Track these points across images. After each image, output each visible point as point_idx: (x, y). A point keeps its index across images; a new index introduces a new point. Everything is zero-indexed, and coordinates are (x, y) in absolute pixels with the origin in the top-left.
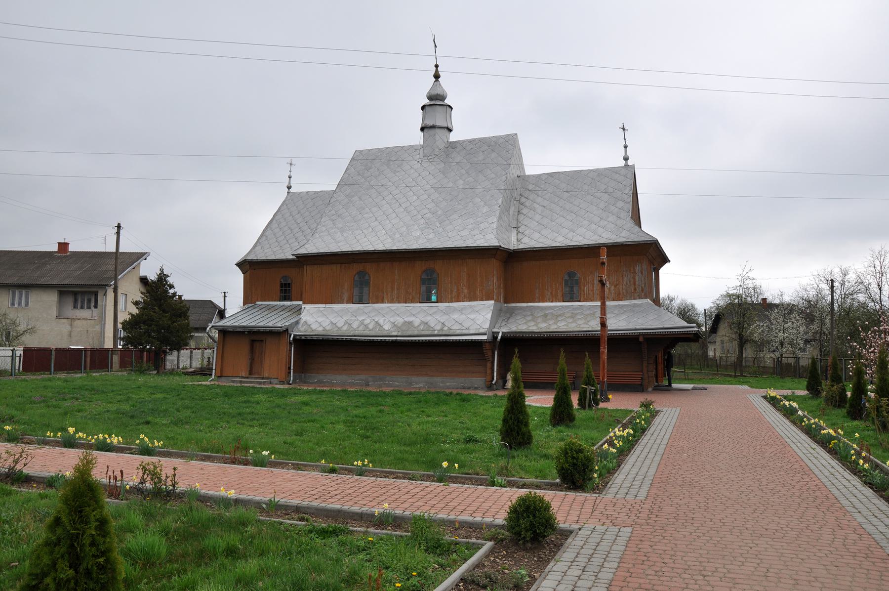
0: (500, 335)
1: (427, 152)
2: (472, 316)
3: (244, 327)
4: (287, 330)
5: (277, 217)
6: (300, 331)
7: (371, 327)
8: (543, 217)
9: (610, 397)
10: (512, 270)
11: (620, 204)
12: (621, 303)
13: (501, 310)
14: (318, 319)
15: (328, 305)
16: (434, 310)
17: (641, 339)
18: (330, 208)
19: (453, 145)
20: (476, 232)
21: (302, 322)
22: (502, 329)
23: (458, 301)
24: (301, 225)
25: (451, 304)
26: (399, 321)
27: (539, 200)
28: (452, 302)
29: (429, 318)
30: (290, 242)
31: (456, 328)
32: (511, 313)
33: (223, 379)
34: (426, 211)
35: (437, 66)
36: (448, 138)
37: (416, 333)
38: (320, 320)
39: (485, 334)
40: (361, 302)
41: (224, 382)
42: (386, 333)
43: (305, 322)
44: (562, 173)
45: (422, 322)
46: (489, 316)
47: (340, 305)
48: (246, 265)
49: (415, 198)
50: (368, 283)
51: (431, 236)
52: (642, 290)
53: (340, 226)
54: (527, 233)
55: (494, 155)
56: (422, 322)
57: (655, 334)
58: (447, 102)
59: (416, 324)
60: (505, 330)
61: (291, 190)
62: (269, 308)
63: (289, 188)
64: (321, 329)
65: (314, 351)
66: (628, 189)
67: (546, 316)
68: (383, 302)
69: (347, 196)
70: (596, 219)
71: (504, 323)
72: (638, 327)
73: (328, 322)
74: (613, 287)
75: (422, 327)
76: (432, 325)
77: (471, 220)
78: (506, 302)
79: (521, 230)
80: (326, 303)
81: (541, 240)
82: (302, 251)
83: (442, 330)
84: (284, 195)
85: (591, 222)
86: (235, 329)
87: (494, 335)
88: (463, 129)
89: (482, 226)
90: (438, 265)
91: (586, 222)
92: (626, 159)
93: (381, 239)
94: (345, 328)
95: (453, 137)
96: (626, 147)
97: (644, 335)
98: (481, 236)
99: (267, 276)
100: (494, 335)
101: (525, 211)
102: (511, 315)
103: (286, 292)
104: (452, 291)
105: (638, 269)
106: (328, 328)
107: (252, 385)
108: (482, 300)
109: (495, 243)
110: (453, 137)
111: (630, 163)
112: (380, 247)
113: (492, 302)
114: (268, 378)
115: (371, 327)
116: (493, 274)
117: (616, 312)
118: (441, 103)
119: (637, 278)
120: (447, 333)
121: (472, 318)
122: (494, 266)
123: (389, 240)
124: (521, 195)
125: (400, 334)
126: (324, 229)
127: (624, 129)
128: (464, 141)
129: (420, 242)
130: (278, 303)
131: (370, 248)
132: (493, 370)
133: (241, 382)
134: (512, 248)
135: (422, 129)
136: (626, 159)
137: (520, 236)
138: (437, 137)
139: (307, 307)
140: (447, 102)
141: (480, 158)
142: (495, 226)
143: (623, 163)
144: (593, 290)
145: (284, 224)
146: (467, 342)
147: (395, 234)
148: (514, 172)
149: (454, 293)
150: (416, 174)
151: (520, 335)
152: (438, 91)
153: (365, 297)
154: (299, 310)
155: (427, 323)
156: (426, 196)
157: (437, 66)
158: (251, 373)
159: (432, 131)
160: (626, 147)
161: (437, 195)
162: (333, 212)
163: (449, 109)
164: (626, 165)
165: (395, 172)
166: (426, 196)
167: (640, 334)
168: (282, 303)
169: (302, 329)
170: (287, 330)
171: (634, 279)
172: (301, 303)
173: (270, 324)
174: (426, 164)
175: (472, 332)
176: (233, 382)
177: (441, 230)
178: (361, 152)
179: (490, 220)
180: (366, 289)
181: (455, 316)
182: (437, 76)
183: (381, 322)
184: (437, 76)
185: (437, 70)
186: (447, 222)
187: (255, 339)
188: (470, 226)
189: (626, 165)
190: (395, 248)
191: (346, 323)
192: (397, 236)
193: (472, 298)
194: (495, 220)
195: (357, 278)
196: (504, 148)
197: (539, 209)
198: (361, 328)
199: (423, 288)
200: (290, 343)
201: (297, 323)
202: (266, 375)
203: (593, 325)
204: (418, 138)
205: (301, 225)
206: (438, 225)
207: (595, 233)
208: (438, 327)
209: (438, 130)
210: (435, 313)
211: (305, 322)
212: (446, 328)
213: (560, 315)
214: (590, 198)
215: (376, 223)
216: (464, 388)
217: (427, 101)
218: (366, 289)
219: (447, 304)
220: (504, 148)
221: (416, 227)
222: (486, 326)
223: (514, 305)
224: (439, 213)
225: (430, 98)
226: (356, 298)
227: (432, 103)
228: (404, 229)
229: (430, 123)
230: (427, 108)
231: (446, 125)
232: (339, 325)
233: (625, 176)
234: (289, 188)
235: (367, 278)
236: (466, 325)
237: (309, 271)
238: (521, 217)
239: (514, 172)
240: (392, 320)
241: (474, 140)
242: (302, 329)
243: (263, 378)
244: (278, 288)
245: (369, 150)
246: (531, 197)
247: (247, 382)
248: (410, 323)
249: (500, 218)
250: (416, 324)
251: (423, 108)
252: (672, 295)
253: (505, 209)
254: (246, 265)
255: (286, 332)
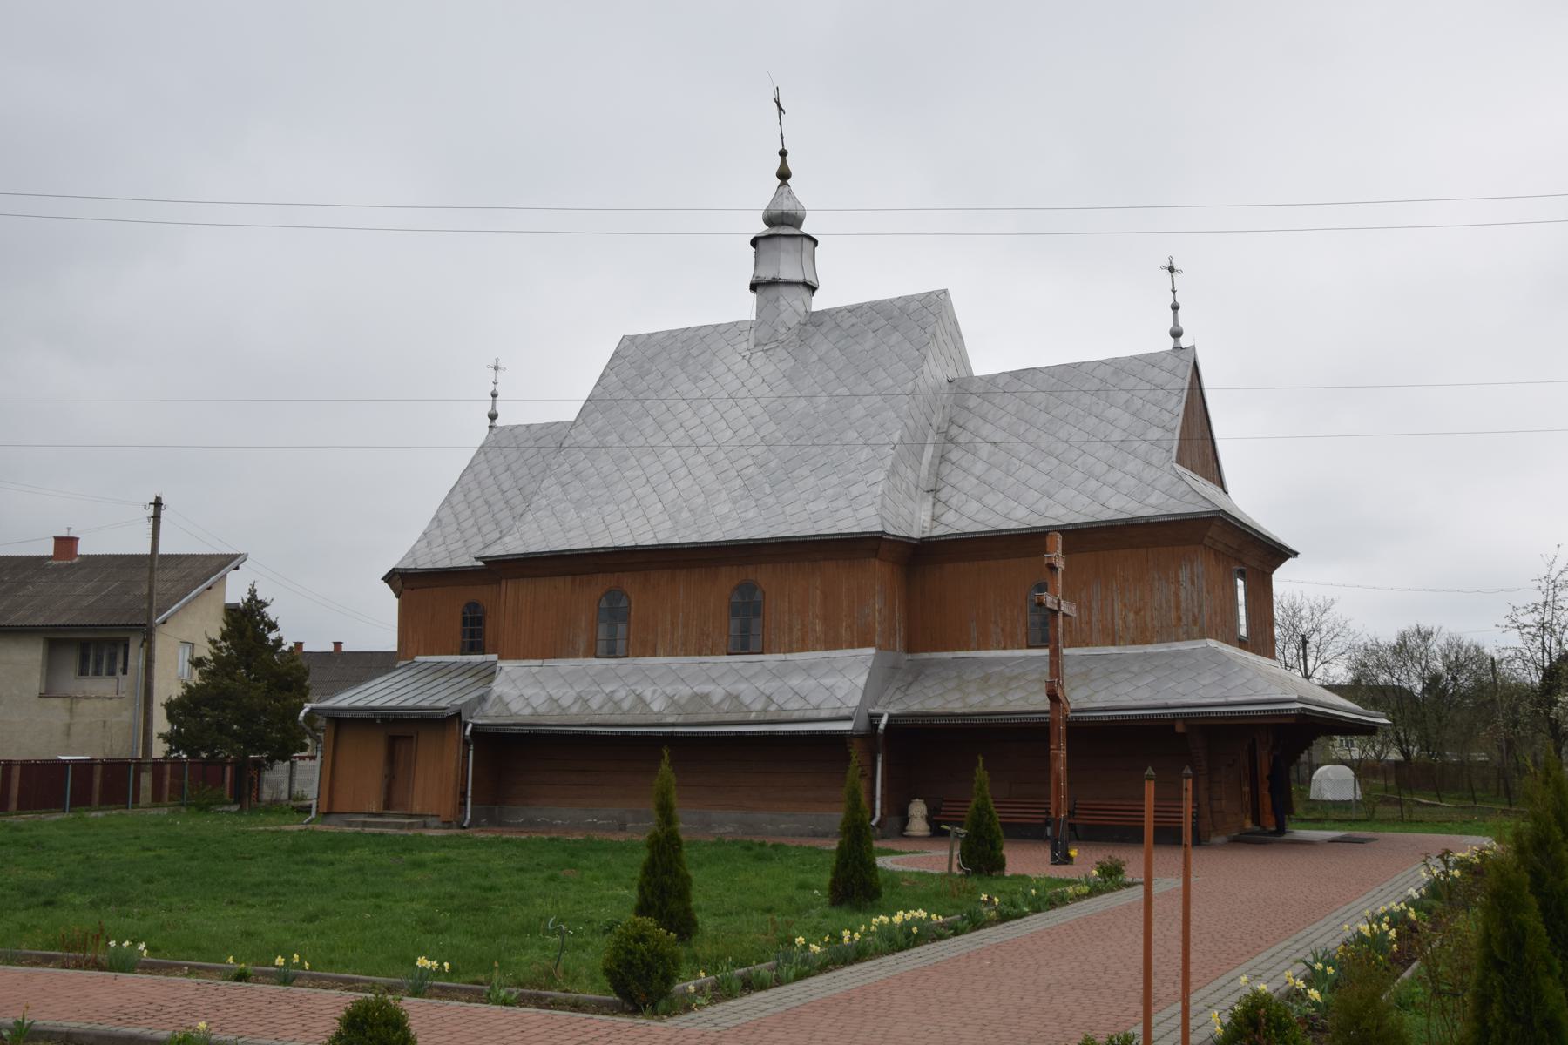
0: (884, 720)
1: (763, 334)
2: (828, 682)
3: (373, 709)
4: (458, 715)
5: (464, 480)
6: (488, 715)
7: (626, 705)
8: (991, 466)
9: (1073, 853)
10: (924, 581)
11: (1154, 433)
12: (1150, 649)
13: (895, 668)
14: (530, 690)
15: (548, 662)
16: (757, 667)
17: (1180, 728)
18: (561, 459)
19: (817, 320)
20: (841, 503)
21: (493, 696)
22: (890, 708)
23: (803, 648)
24: (509, 495)
25: (789, 656)
26: (684, 691)
27: (987, 430)
28: (791, 651)
29: (742, 687)
30: (484, 530)
31: (794, 707)
32: (918, 673)
33: (333, 819)
34: (749, 461)
35: (783, 153)
36: (807, 305)
37: (713, 718)
38: (528, 692)
39: (848, 719)
40: (611, 654)
41: (332, 827)
42: (653, 719)
43: (500, 697)
44: (1041, 370)
45: (729, 695)
46: (862, 681)
47: (572, 662)
48: (399, 579)
49: (729, 433)
50: (626, 618)
51: (751, 514)
52: (1195, 621)
53: (576, 495)
54: (954, 502)
55: (895, 338)
56: (729, 695)
57: (1207, 716)
58: (806, 228)
59: (716, 699)
60: (895, 709)
61: (498, 422)
62: (437, 669)
63: (493, 417)
64: (527, 711)
65: (518, 759)
66: (1175, 400)
67: (986, 678)
68: (654, 654)
69: (595, 433)
70: (1100, 468)
71: (898, 695)
72: (1171, 702)
73: (543, 696)
74: (1131, 616)
75: (725, 706)
76: (747, 701)
77: (834, 479)
78: (910, 648)
79: (942, 495)
80: (543, 658)
81: (981, 517)
82: (496, 550)
83: (765, 711)
84: (481, 432)
85: (1089, 475)
86: (355, 714)
87: (874, 719)
88: (845, 278)
89: (855, 491)
90: (764, 576)
91: (1077, 476)
92: (1176, 334)
93: (653, 522)
94: (575, 709)
95: (819, 302)
96: (1175, 308)
97: (1186, 719)
98: (849, 512)
99: (452, 601)
100: (874, 719)
101: (955, 455)
102: (916, 678)
103: (475, 635)
104: (791, 628)
105: (1184, 574)
106: (541, 710)
107: (377, 830)
108: (851, 646)
109: (874, 526)
110: (819, 302)
111: (1185, 342)
112: (647, 540)
113: (871, 651)
114: (421, 816)
115: (626, 705)
116: (875, 590)
117: (1135, 669)
118: (796, 232)
119: (1183, 594)
120: (775, 717)
121: (826, 684)
122: (878, 574)
123: (668, 524)
124: (951, 421)
125: (681, 720)
126: (544, 502)
127: (1171, 270)
128: (839, 310)
129: (728, 526)
130: (458, 658)
131: (626, 540)
132: (874, 796)
133: (365, 824)
134: (916, 533)
135: (754, 287)
136: (1176, 334)
137: (940, 509)
138: (782, 302)
139: (508, 666)
140: (806, 228)
141: (868, 346)
142: (879, 489)
143: (1169, 343)
144: (1089, 622)
145: (474, 494)
146: (812, 736)
147: (680, 511)
148: (938, 372)
149: (796, 634)
150: (737, 384)
151: (926, 721)
152: (787, 206)
153: (621, 645)
154: (489, 673)
155: (737, 697)
156: (750, 430)
157: (783, 153)
158: (388, 804)
159: (771, 292)
160: (1175, 308)
161: (772, 427)
162: (566, 467)
163: (808, 244)
164: (1177, 348)
165: (695, 380)
166: (750, 430)
167: (1176, 718)
168: (465, 658)
169: (492, 712)
170: (458, 715)
171: (1177, 595)
172: (494, 657)
173: (425, 704)
174: (759, 358)
175: (823, 714)
176: (350, 824)
177: (771, 500)
178: (633, 338)
179: (872, 477)
180: (622, 628)
181: (795, 681)
182: (784, 175)
183: (648, 695)
184: (784, 175)
185: (784, 162)
186: (787, 483)
187: (400, 732)
188: (830, 492)
189: (1177, 348)
190: (676, 540)
191: (579, 698)
192: (685, 514)
193: (832, 642)
194: (882, 476)
195: (604, 604)
196: (922, 320)
197: (985, 450)
198: (605, 710)
199: (735, 624)
200: (466, 743)
201: (482, 699)
202: (417, 809)
203: (1028, 699)
204: (745, 307)
205: (509, 495)
206: (768, 490)
207: (1093, 497)
208: (758, 706)
209: (784, 290)
210: (755, 675)
211: (500, 697)
212: (773, 708)
213: (1016, 677)
214: (1091, 422)
215: (648, 489)
216: (815, 835)
217: (762, 229)
218: (622, 628)
219: (781, 656)
220: (922, 320)
221: (724, 495)
222: (855, 701)
223: (926, 655)
224: (773, 464)
225: (770, 221)
226: (602, 646)
227: (773, 231)
228: (700, 500)
229: (767, 274)
230: (761, 243)
231: (800, 277)
232: (565, 702)
233: (1172, 372)
234: (493, 417)
235: (623, 604)
236: (814, 701)
237: (513, 593)
238: (946, 469)
239: (937, 372)
240: (669, 690)
241: (860, 306)
242: (492, 712)
243: (410, 816)
244: (457, 625)
245: (650, 335)
246: (970, 425)
247: (376, 825)
248: (705, 697)
249: (893, 472)
250: (716, 699)
251: (754, 242)
252: (1426, 625)
253: (912, 447)
254: (399, 579)
255: (453, 719)
